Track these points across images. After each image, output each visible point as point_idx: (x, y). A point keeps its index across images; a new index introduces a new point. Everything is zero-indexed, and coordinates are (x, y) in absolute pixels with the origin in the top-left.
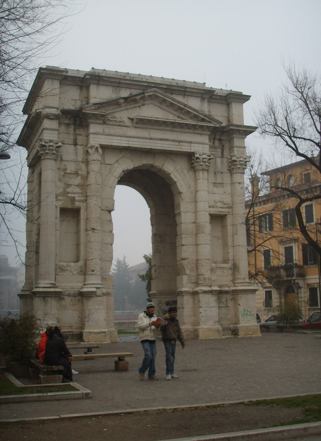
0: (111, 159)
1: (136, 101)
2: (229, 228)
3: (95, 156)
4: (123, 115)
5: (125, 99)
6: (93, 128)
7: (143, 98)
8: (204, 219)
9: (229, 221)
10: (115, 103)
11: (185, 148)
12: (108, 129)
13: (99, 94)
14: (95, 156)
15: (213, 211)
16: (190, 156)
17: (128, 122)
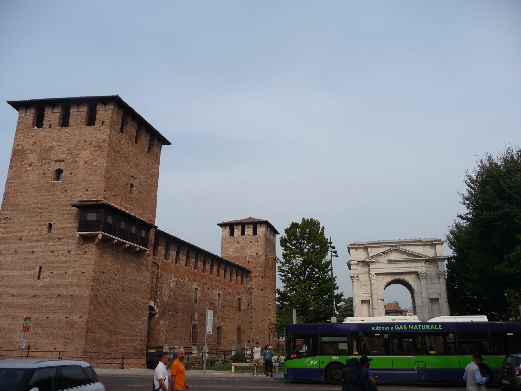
0: (380, 278)
1: (387, 253)
2: (441, 304)
3: (374, 278)
4: (383, 259)
5: (383, 253)
6: (371, 266)
7: (391, 251)
8: (426, 301)
9: (440, 300)
10: (379, 255)
11: (413, 270)
12: (377, 266)
13: (373, 252)
14: (374, 278)
15: (431, 297)
16: (416, 273)
17: (386, 262)
